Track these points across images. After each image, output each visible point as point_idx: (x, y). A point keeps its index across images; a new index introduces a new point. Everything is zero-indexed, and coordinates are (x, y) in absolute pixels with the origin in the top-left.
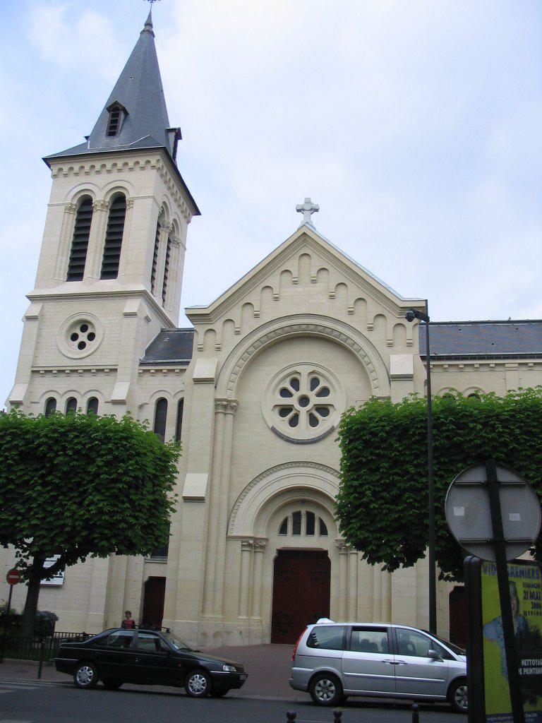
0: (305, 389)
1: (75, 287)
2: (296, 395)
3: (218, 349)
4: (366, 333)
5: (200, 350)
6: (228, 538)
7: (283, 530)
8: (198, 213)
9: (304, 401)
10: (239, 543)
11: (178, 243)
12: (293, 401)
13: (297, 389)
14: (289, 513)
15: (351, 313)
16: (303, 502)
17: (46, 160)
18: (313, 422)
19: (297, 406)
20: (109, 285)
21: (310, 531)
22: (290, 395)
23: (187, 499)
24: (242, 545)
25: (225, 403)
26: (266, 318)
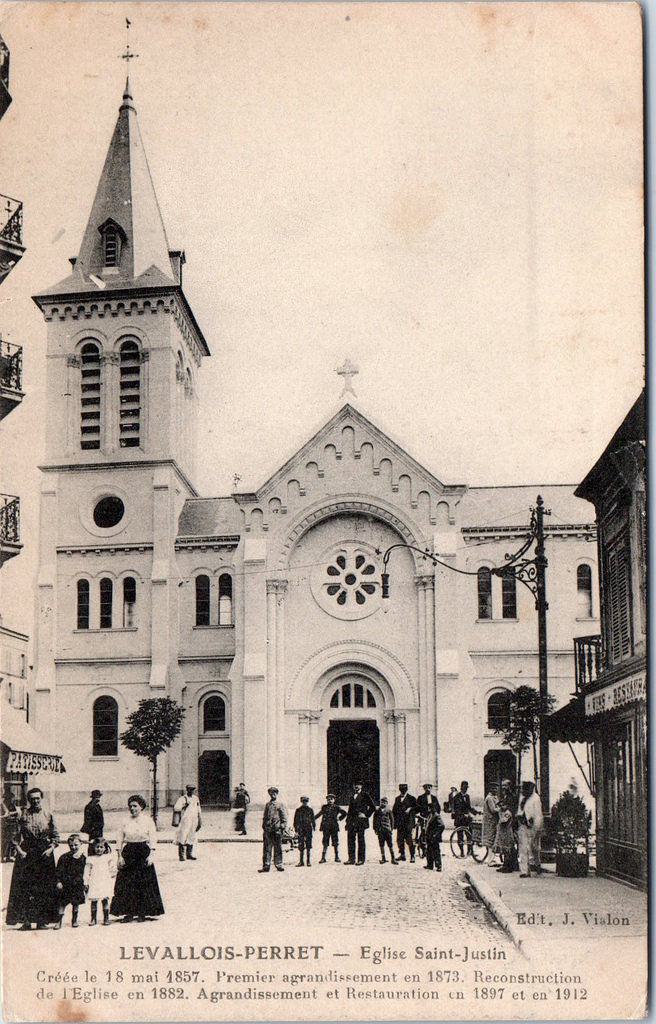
0: (351, 567)
1: (92, 457)
2: (344, 573)
7: (334, 703)
8: (209, 354)
9: (351, 579)
14: (338, 686)
17: (35, 299)
18: (360, 599)
19: (344, 585)
20: (131, 454)
22: (338, 573)
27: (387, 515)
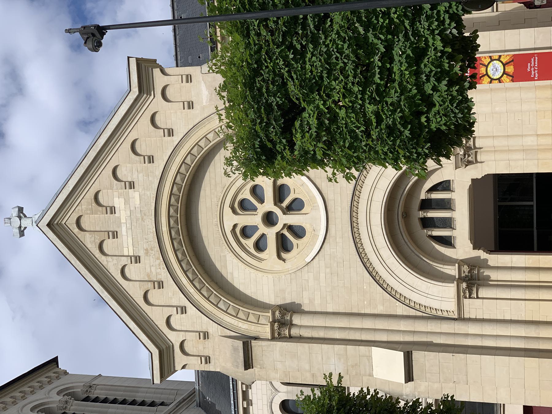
2: (263, 229)
3: (206, 335)
4: (176, 139)
5: (208, 360)
6: (461, 319)
7: (447, 242)
10: (466, 302)
11: (90, 387)
12: (271, 233)
13: (255, 228)
15: (151, 159)
16: (406, 215)
19: (278, 228)
21: (446, 205)
23: (409, 377)
24: (470, 298)
25: (276, 324)
26: (164, 276)
27: (183, 170)
